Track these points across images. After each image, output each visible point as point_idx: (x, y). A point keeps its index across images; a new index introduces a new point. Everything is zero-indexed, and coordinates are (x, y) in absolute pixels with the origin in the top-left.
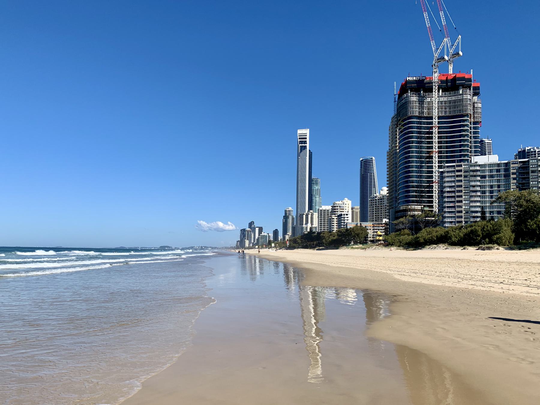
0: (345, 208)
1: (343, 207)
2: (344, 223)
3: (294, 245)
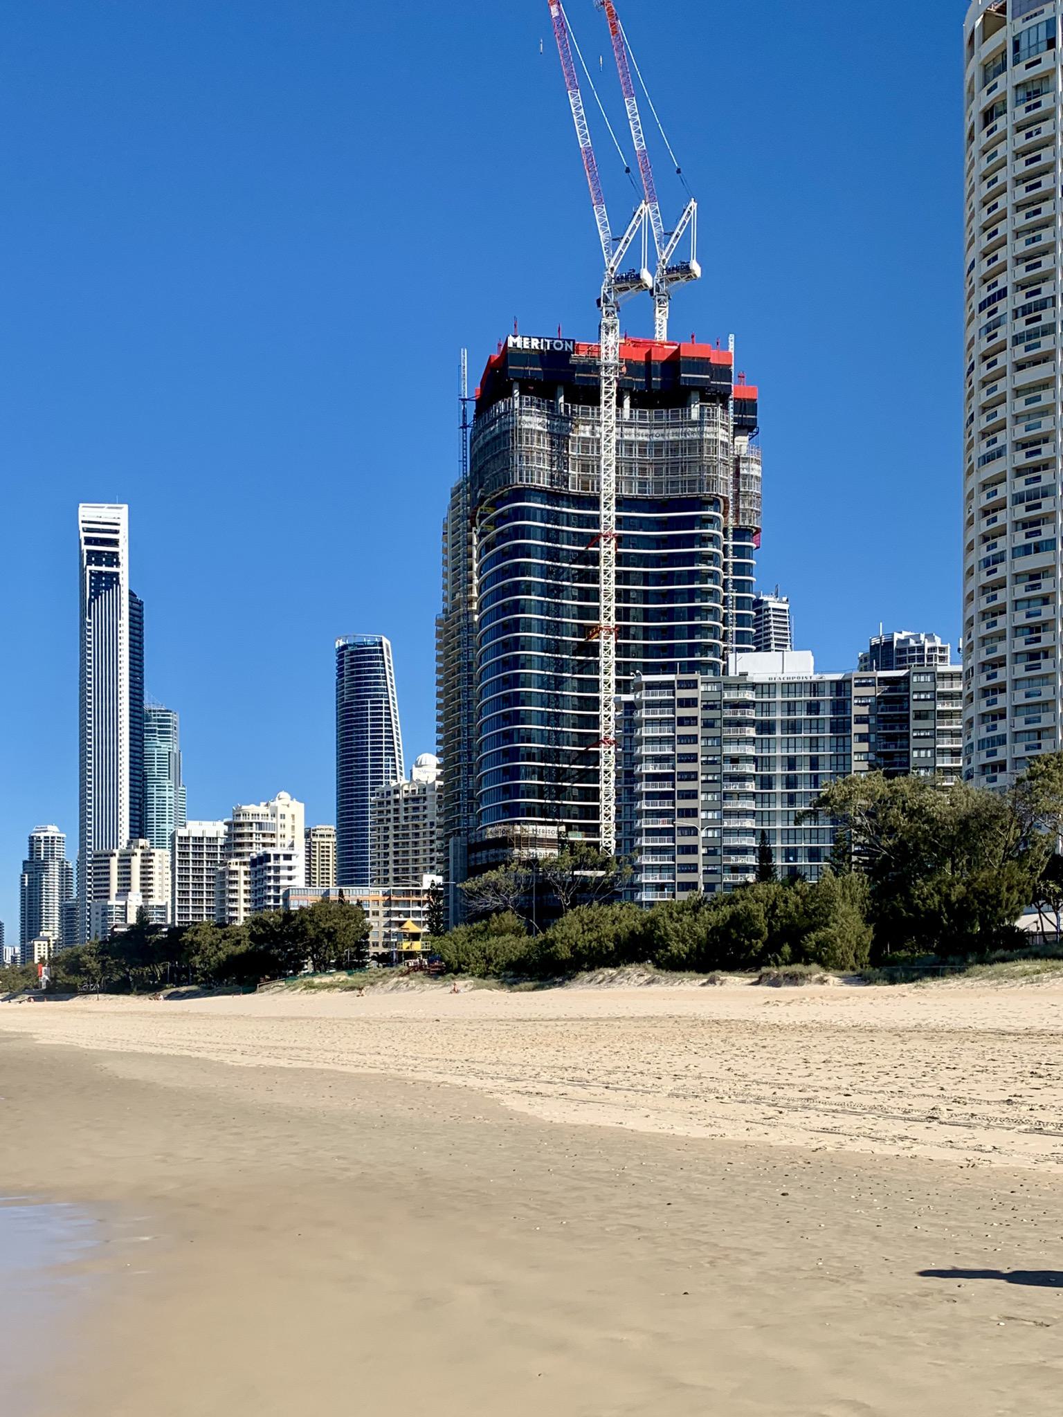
2: (277, 889)
3: (68, 980)
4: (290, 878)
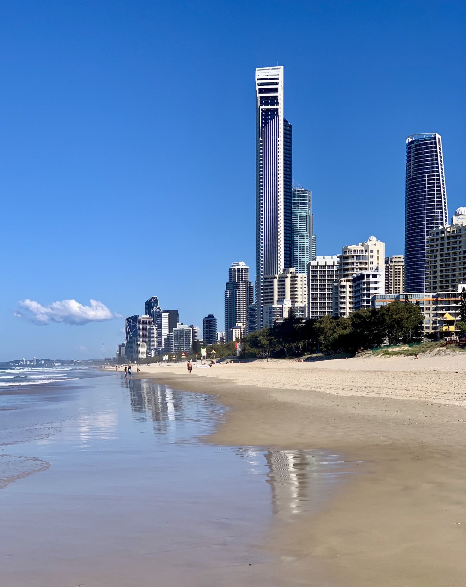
0: (370, 260)
1: (366, 257)
3: (252, 350)
4: (376, 289)
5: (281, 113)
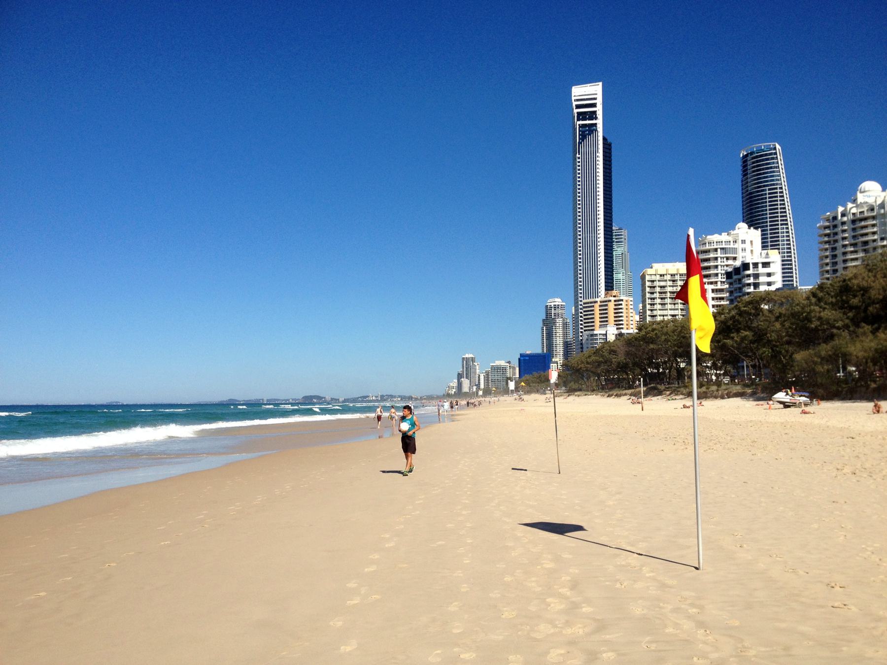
1: (735, 250)
5: (600, 128)
